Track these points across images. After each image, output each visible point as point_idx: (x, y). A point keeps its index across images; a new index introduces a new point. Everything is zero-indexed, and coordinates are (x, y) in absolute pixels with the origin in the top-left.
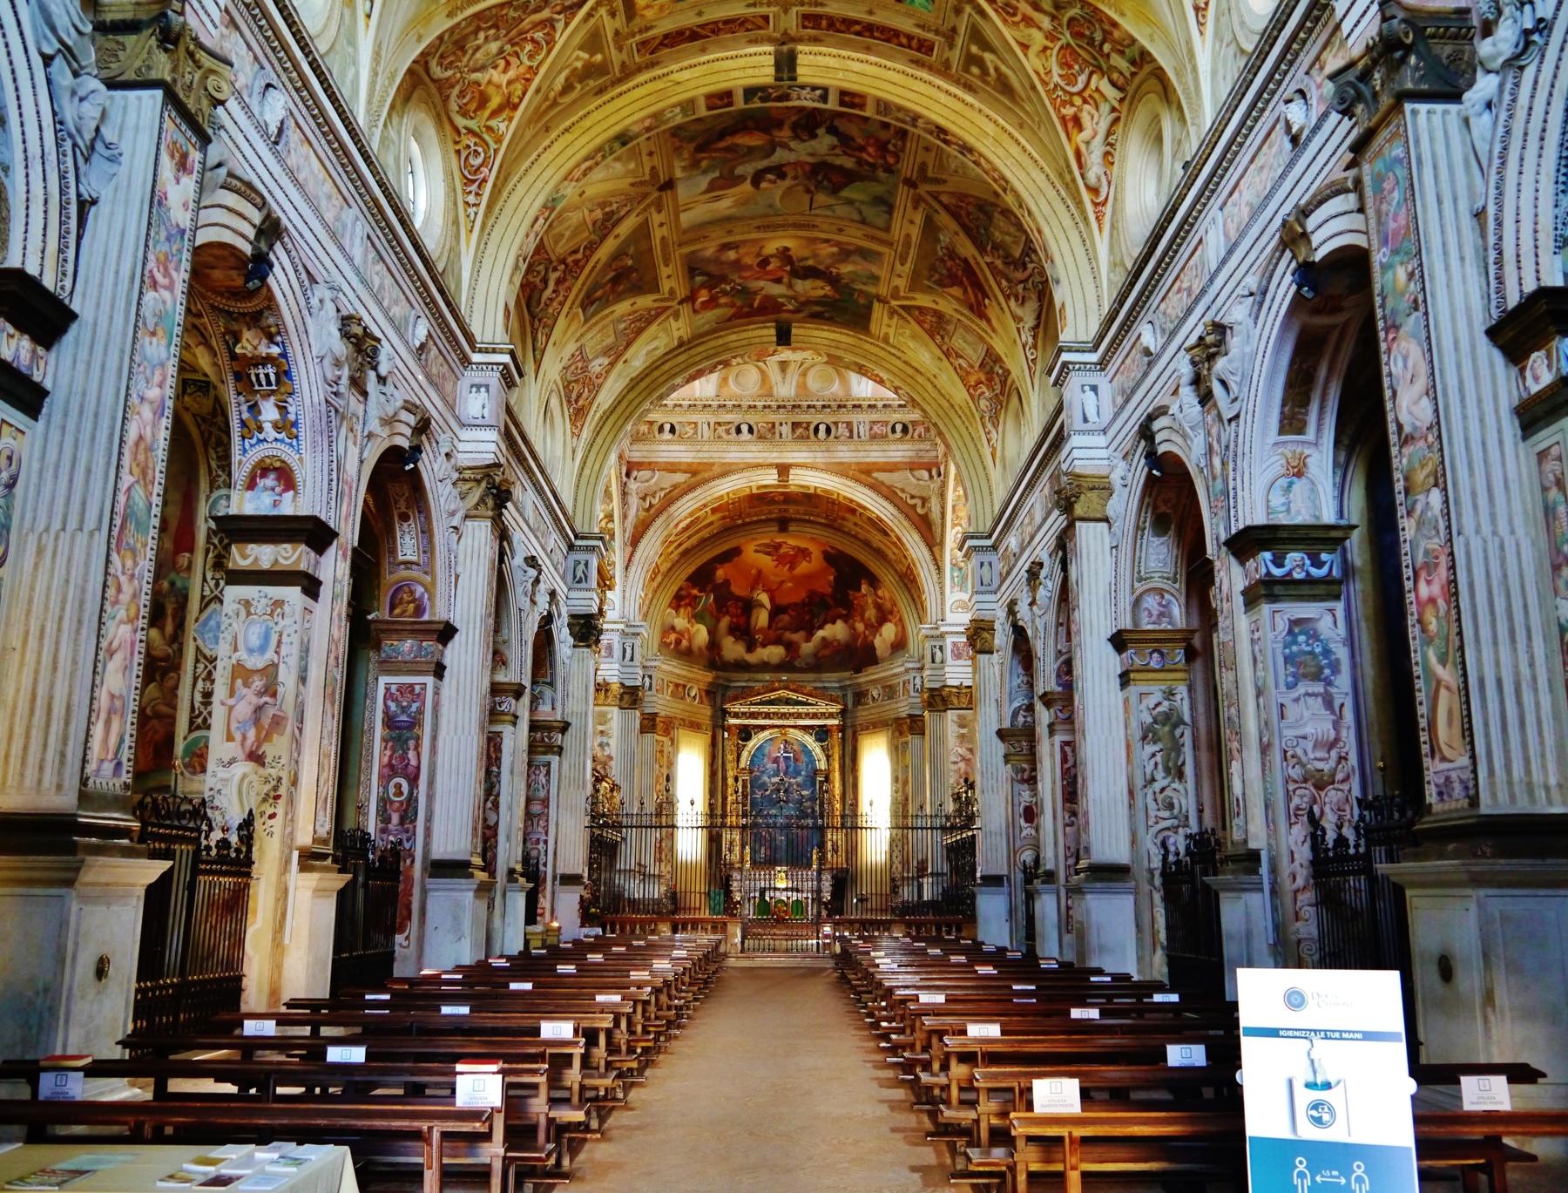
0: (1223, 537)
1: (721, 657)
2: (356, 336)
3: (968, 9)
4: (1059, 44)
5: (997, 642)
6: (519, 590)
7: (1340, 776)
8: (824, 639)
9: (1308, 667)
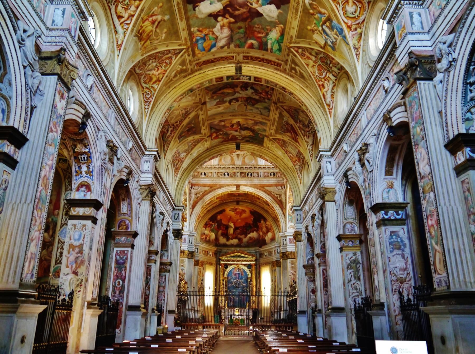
0: (369, 206)
1: (219, 243)
2: (111, 146)
3: (291, 54)
4: (317, 64)
5: (302, 238)
6: (158, 222)
7: (408, 279)
8: (250, 237)
9: (396, 246)
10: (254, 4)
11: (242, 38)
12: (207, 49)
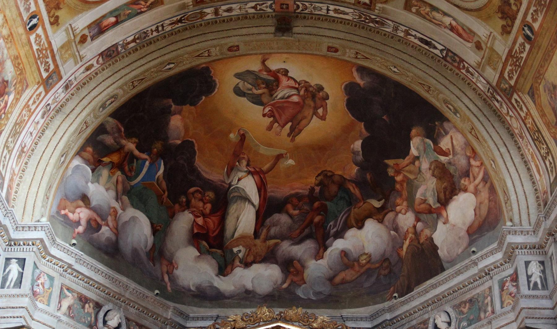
8: (344, 253)
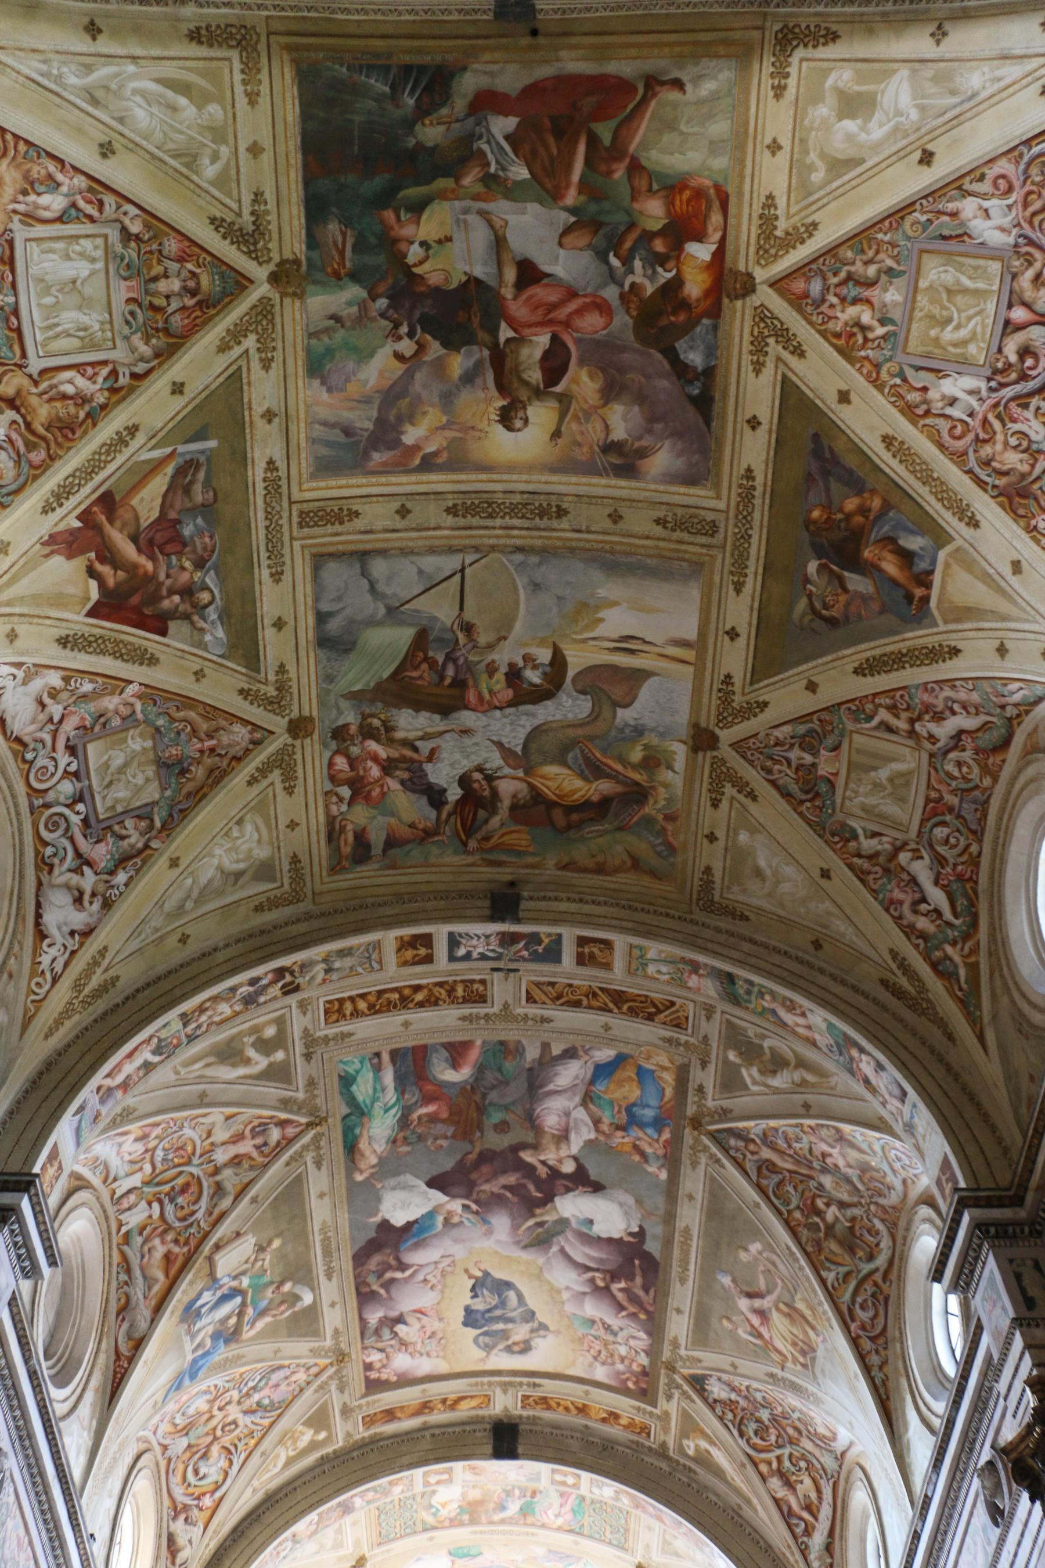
4: (198, 1152)
10: (459, 1210)
11: (493, 1087)
12: (631, 1072)
